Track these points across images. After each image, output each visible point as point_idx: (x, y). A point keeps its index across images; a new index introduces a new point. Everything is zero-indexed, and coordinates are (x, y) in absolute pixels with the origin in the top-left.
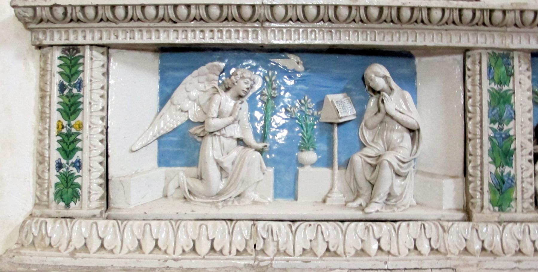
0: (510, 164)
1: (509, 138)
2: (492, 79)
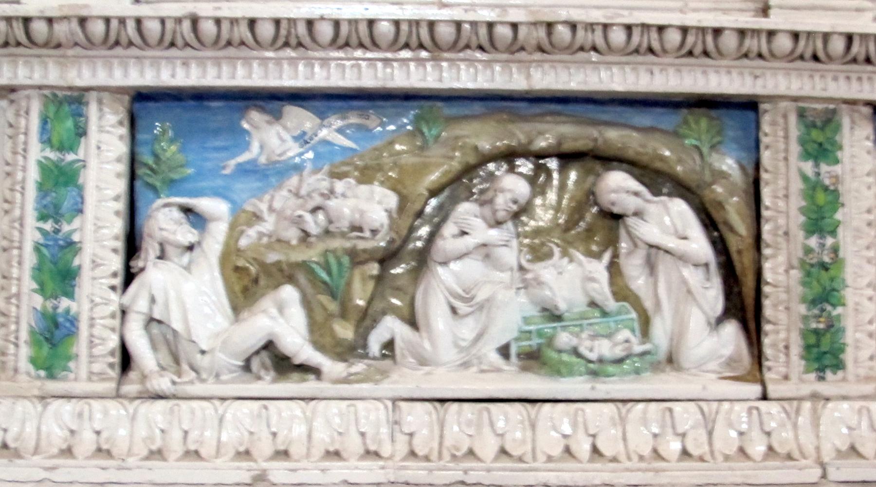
0: (70, 295)
1: (71, 246)
2: (47, 141)
